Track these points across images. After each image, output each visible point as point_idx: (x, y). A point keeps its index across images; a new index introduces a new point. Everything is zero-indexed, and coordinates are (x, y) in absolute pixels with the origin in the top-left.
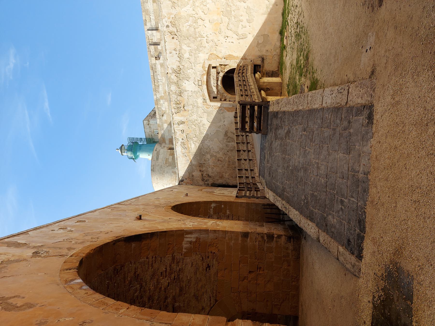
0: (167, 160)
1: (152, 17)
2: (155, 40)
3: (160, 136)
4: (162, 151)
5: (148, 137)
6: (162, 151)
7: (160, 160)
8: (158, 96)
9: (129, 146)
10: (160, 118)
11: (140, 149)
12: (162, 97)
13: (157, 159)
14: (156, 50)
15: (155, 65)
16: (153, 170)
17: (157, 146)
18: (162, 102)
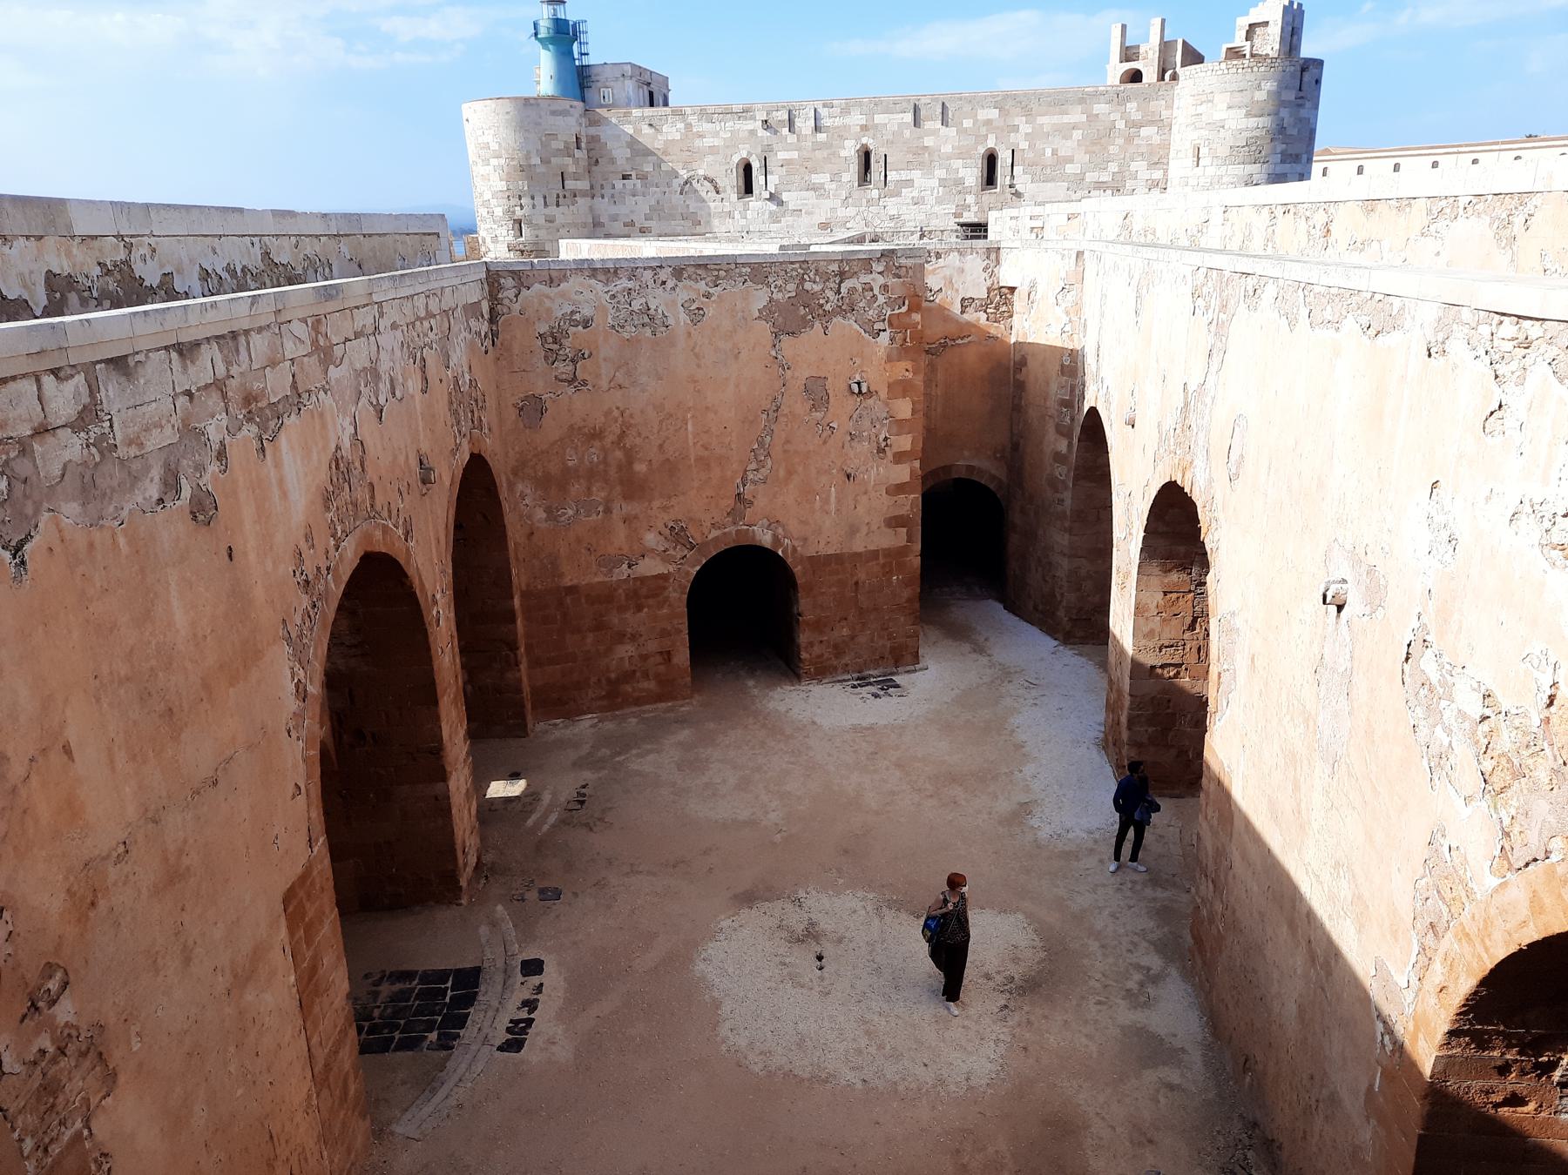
0: (553, 136)
1: (838, 122)
2: (798, 123)
3: (602, 112)
4: (572, 121)
5: (593, 71)
6: (572, 121)
7: (552, 120)
8: (692, 119)
9: (566, 21)
10: (643, 118)
11: (563, 54)
12: (689, 126)
13: (554, 113)
15: (753, 118)
16: (527, 102)
18: (681, 126)
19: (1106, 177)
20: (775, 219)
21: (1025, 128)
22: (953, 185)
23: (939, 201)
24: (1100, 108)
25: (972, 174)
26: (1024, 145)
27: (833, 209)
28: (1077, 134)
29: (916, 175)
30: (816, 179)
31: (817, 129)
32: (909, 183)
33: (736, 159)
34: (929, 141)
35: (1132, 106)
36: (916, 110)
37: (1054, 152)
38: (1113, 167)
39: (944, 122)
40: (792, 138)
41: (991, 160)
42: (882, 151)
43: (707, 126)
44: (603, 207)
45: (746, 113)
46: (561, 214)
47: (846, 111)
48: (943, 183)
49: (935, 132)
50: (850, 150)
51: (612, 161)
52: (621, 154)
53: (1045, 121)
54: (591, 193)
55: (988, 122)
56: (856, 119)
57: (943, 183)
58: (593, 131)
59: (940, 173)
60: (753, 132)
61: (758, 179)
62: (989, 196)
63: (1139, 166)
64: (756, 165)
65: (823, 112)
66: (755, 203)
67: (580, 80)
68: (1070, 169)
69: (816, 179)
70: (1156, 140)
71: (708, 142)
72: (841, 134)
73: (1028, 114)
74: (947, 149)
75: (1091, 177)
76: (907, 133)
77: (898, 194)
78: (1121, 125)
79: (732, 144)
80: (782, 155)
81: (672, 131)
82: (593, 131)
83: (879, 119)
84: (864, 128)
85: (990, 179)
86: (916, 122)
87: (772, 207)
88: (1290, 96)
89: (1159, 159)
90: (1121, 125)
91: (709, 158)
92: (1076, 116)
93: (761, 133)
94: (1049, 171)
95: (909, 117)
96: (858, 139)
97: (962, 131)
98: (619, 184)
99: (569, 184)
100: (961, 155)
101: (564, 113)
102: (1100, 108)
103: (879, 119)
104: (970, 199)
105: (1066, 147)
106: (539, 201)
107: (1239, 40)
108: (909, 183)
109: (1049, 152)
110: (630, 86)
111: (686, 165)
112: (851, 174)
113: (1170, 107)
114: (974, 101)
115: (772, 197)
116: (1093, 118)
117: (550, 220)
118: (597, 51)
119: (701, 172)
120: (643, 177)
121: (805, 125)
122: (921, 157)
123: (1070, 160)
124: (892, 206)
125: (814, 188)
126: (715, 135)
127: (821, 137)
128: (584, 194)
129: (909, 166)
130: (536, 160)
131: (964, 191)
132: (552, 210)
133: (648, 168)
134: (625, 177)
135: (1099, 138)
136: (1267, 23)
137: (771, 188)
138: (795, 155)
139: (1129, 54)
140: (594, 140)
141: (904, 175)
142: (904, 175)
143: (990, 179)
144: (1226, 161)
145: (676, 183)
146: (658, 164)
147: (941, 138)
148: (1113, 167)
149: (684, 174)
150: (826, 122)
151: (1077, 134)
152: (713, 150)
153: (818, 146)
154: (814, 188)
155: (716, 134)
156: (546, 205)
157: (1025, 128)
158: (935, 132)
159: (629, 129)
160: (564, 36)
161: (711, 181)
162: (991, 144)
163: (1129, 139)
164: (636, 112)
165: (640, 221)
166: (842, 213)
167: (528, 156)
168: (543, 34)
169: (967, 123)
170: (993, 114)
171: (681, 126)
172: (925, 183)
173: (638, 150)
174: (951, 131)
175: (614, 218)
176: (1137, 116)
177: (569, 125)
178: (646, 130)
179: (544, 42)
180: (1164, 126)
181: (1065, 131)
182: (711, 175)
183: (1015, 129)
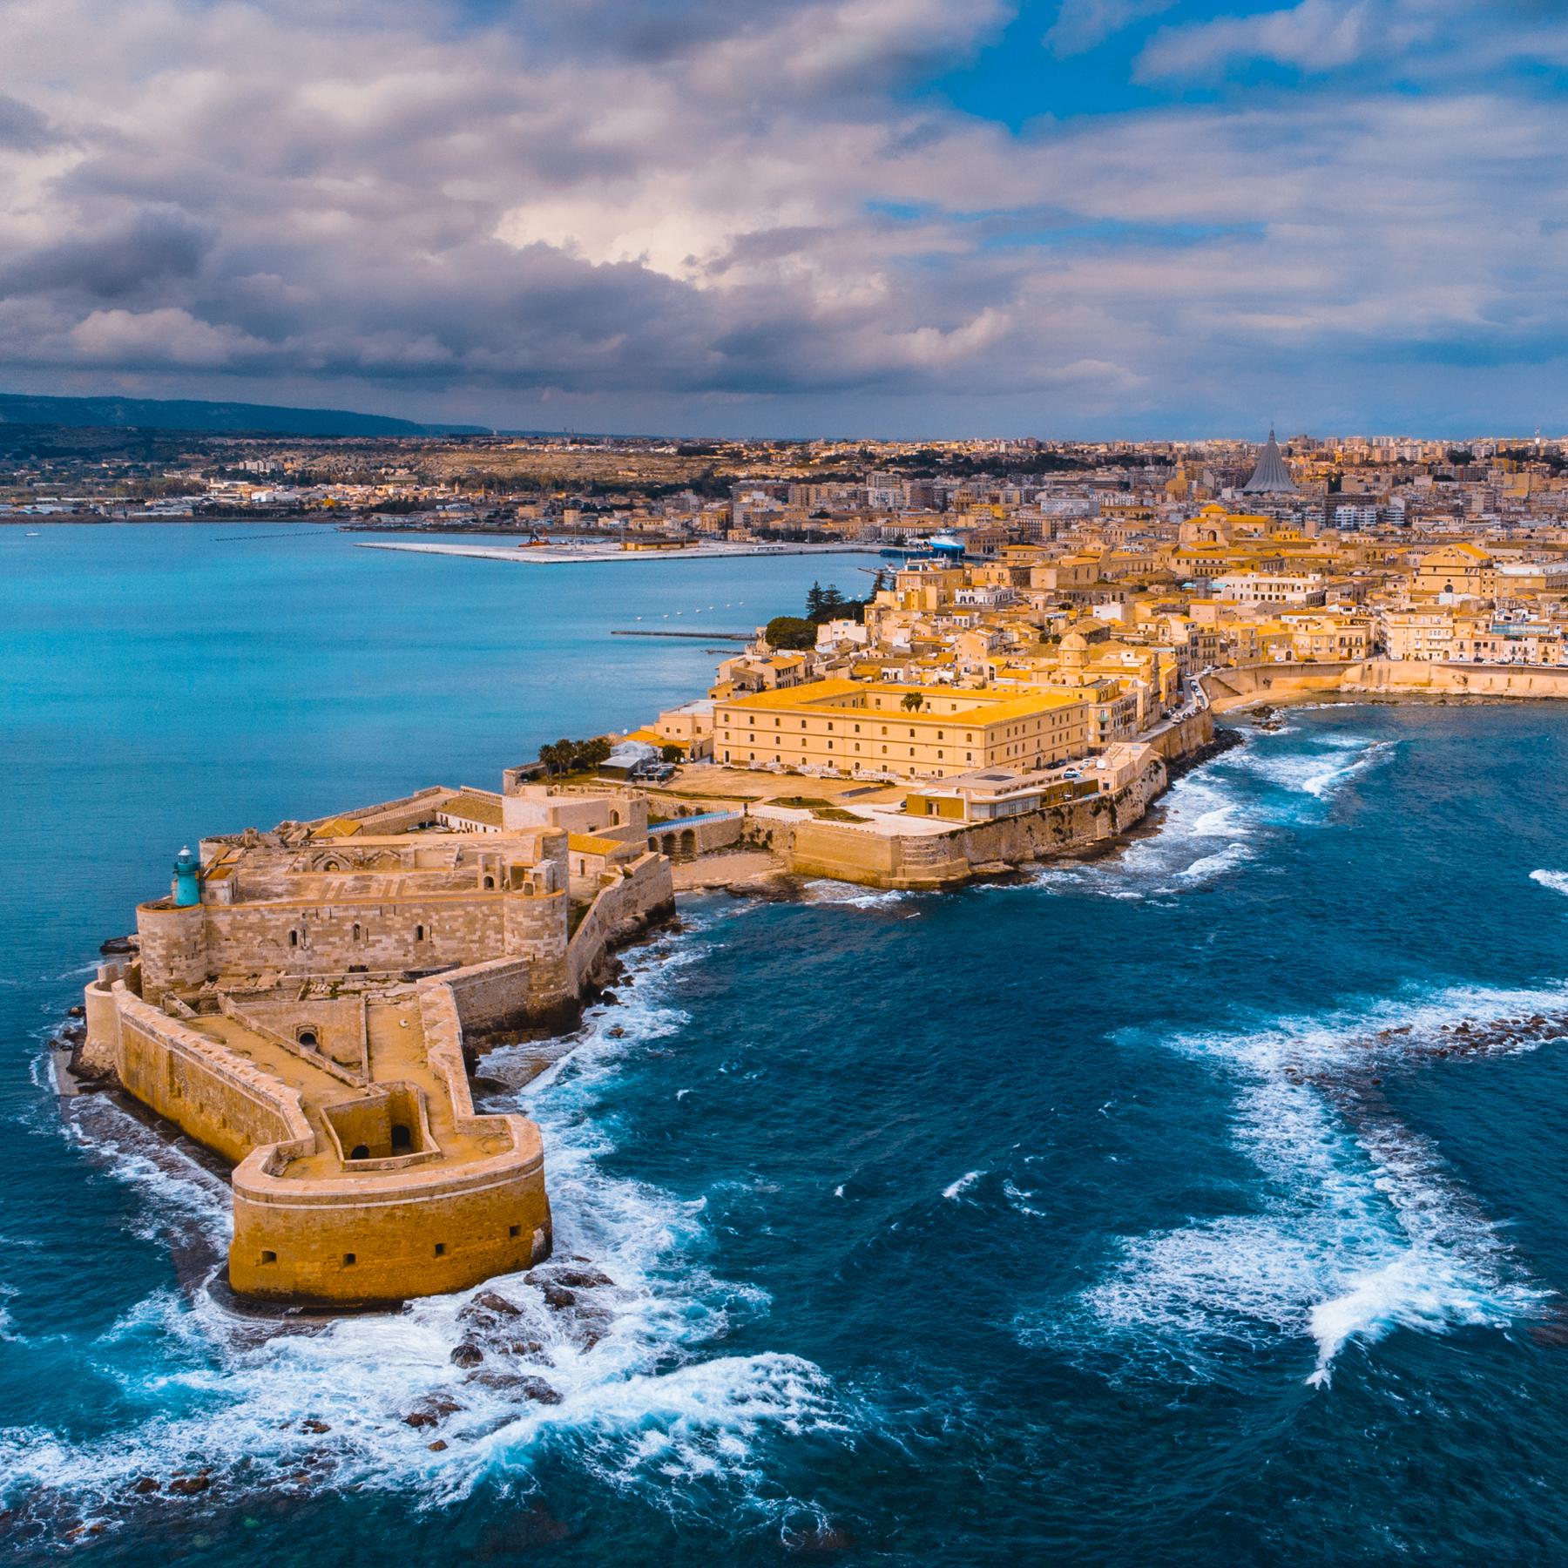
19: (475, 937)
22: (402, 942)
24: (470, 909)
41: (420, 929)
47: (346, 909)
50: (348, 926)
56: (353, 913)
63: (490, 933)
64: (299, 933)
72: (342, 920)
73: (438, 912)
79: (287, 923)
89: (500, 930)
92: (459, 912)
98: (223, 943)
100: (407, 928)
102: (470, 909)
105: (456, 925)
116: (467, 913)
120: (237, 940)
122: (386, 930)
124: (371, 952)
140: (210, 922)
147: (397, 921)
152: (276, 927)
165: (234, 959)
166: (346, 955)
172: (388, 941)
181: (455, 918)
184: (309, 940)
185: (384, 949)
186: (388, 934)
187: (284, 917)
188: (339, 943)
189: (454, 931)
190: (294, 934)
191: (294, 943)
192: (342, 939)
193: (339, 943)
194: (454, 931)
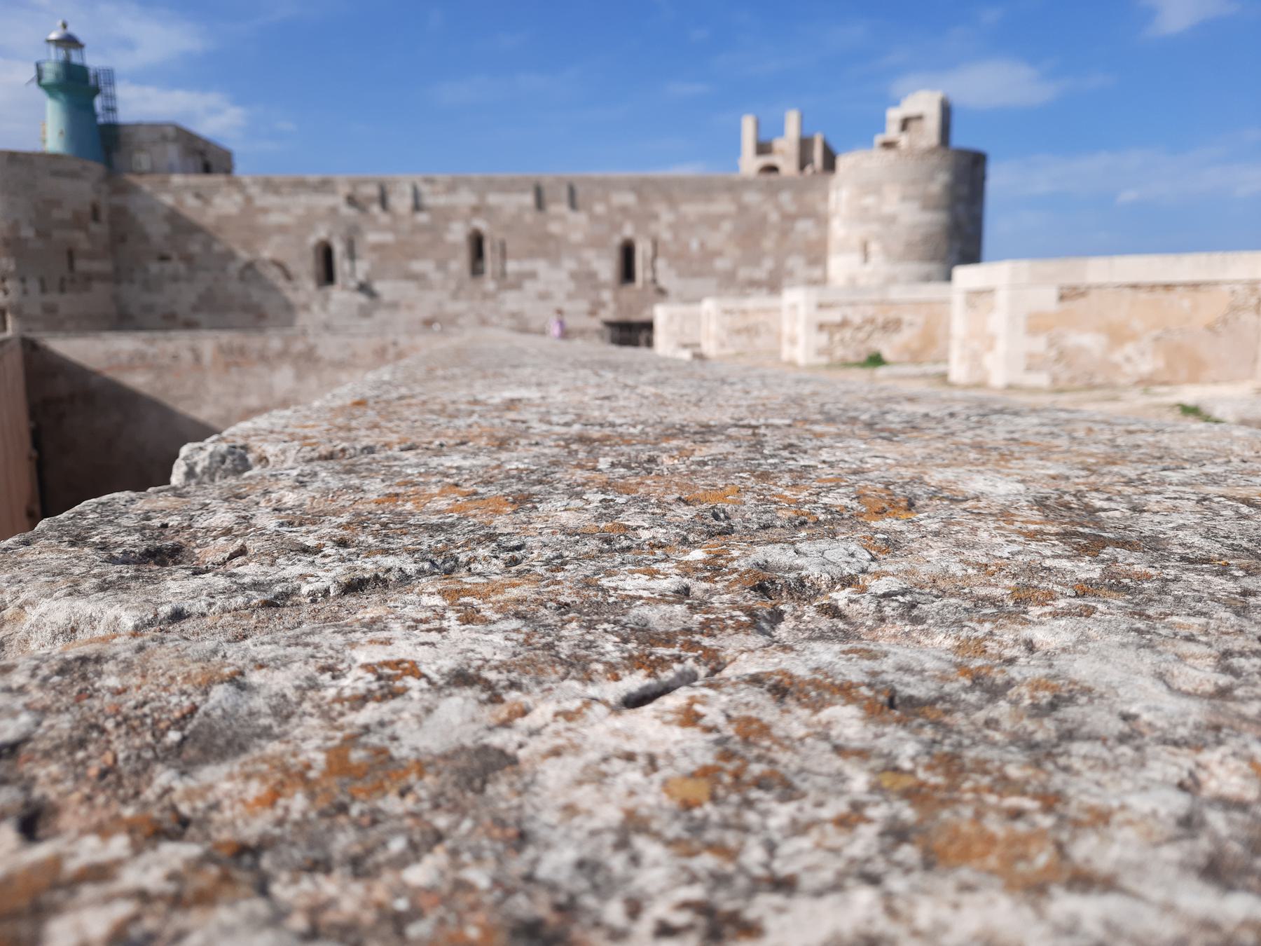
0: (57, 204)
1: (442, 200)
2: (393, 200)
8: (254, 190)
10: (187, 187)
12: (249, 200)
13: (56, 174)
14: (370, 200)
15: (333, 192)
17: (97, 169)
18: (238, 198)
19: (761, 273)
20: (365, 312)
21: (666, 216)
22: (585, 278)
23: (570, 297)
24: (751, 198)
25: (607, 268)
26: (666, 236)
27: (440, 304)
28: (727, 226)
29: (541, 266)
30: (418, 266)
31: (417, 207)
32: (532, 275)
33: (312, 240)
34: (555, 228)
35: (785, 198)
36: (539, 193)
37: (702, 245)
38: (768, 264)
39: (573, 205)
40: (384, 219)
41: (628, 252)
42: (499, 236)
43: (270, 200)
44: (133, 295)
45: (325, 186)
46: (66, 302)
47: (452, 188)
48: (574, 276)
49: (561, 218)
50: (458, 234)
51: (145, 238)
52: (157, 230)
53: (691, 210)
54: (116, 277)
55: (624, 210)
56: (465, 198)
57: (574, 276)
58: (117, 200)
59: (569, 264)
60: (333, 210)
61: (341, 265)
62: (628, 293)
64: (339, 249)
65: (424, 188)
66: (340, 295)
67: (104, 140)
68: (721, 264)
69: (418, 266)
70: (814, 235)
71: (275, 218)
72: (445, 216)
73: (672, 203)
74: (576, 237)
75: (744, 273)
76: (529, 217)
77: (517, 285)
78: (774, 217)
79: (308, 222)
80: (373, 237)
81: (225, 204)
82: (117, 200)
83: (493, 199)
84: (476, 210)
85: (627, 272)
86: (540, 204)
87: (362, 299)
88: (964, 190)
90: (774, 217)
91: (277, 239)
92: (723, 205)
93: (346, 211)
94: (698, 266)
95: (529, 199)
96: (467, 220)
97: (594, 218)
98: (154, 267)
99: (82, 265)
100: (596, 243)
101: (74, 175)
103: (493, 199)
104: (606, 295)
105: (716, 239)
106: (33, 285)
107: (892, 132)
108: (532, 275)
109: (695, 245)
110: (173, 152)
111: (247, 245)
112: (460, 263)
113: (826, 198)
114: (608, 186)
115: (364, 288)
116: (743, 209)
117: (50, 310)
118: (134, 104)
119: (267, 254)
120: (188, 259)
121: (401, 202)
123: (719, 254)
124: (511, 301)
125: (417, 278)
126: (282, 211)
127: (423, 218)
128: (103, 277)
129: (532, 255)
130: (27, 232)
131: (598, 286)
132: (53, 297)
133: (195, 248)
134: (164, 258)
135: (750, 234)
136: (919, 118)
137: (360, 276)
138: (388, 238)
139: (763, 148)
140: (119, 214)
141: (527, 265)
142: (527, 265)
143: (627, 272)
144: (902, 258)
145: (234, 268)
146: (207, 246)
147: (571, 225)
148: (768, 264)
149: (244, 255)
150: (428, 200)
151: (727, 226)
152: (282, 229)
153: (418, 229)
154: (417, 278)
155: (285, 210)
156: (44, 290)
157: (666, 216)
158: (561, 218)
159: (168, 199)
160: (76, 85)
161: (280, 265)
162: (628, 231)
163: (785, 234)
164: (177, 179)
167: (15, 226)
168: (49, 77)
169: (599, 209)
170: (629, 199)
171: (238, 198)
172: (553, 277)
173: (181, 226)
174: (580, 218)
175: (148, 309)
176: (791, 208)
177: (82, 191)
178: (191, 202)
179: (51, 89)
180: (822, 220)
181: (713, 222)
182: (280, 257)
183: (655, 217)
184: (362, 268)
185: (544, 296)
186: (554, 259)
187: (301, 202)
188: (435, 276)
189: (709, 255)
190: (326, 254)
191: (327, 275)
192: (442, 265)
193: (435, 276)
194: (709, 255)
